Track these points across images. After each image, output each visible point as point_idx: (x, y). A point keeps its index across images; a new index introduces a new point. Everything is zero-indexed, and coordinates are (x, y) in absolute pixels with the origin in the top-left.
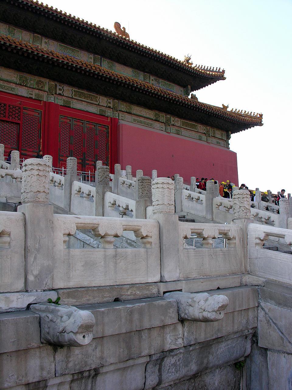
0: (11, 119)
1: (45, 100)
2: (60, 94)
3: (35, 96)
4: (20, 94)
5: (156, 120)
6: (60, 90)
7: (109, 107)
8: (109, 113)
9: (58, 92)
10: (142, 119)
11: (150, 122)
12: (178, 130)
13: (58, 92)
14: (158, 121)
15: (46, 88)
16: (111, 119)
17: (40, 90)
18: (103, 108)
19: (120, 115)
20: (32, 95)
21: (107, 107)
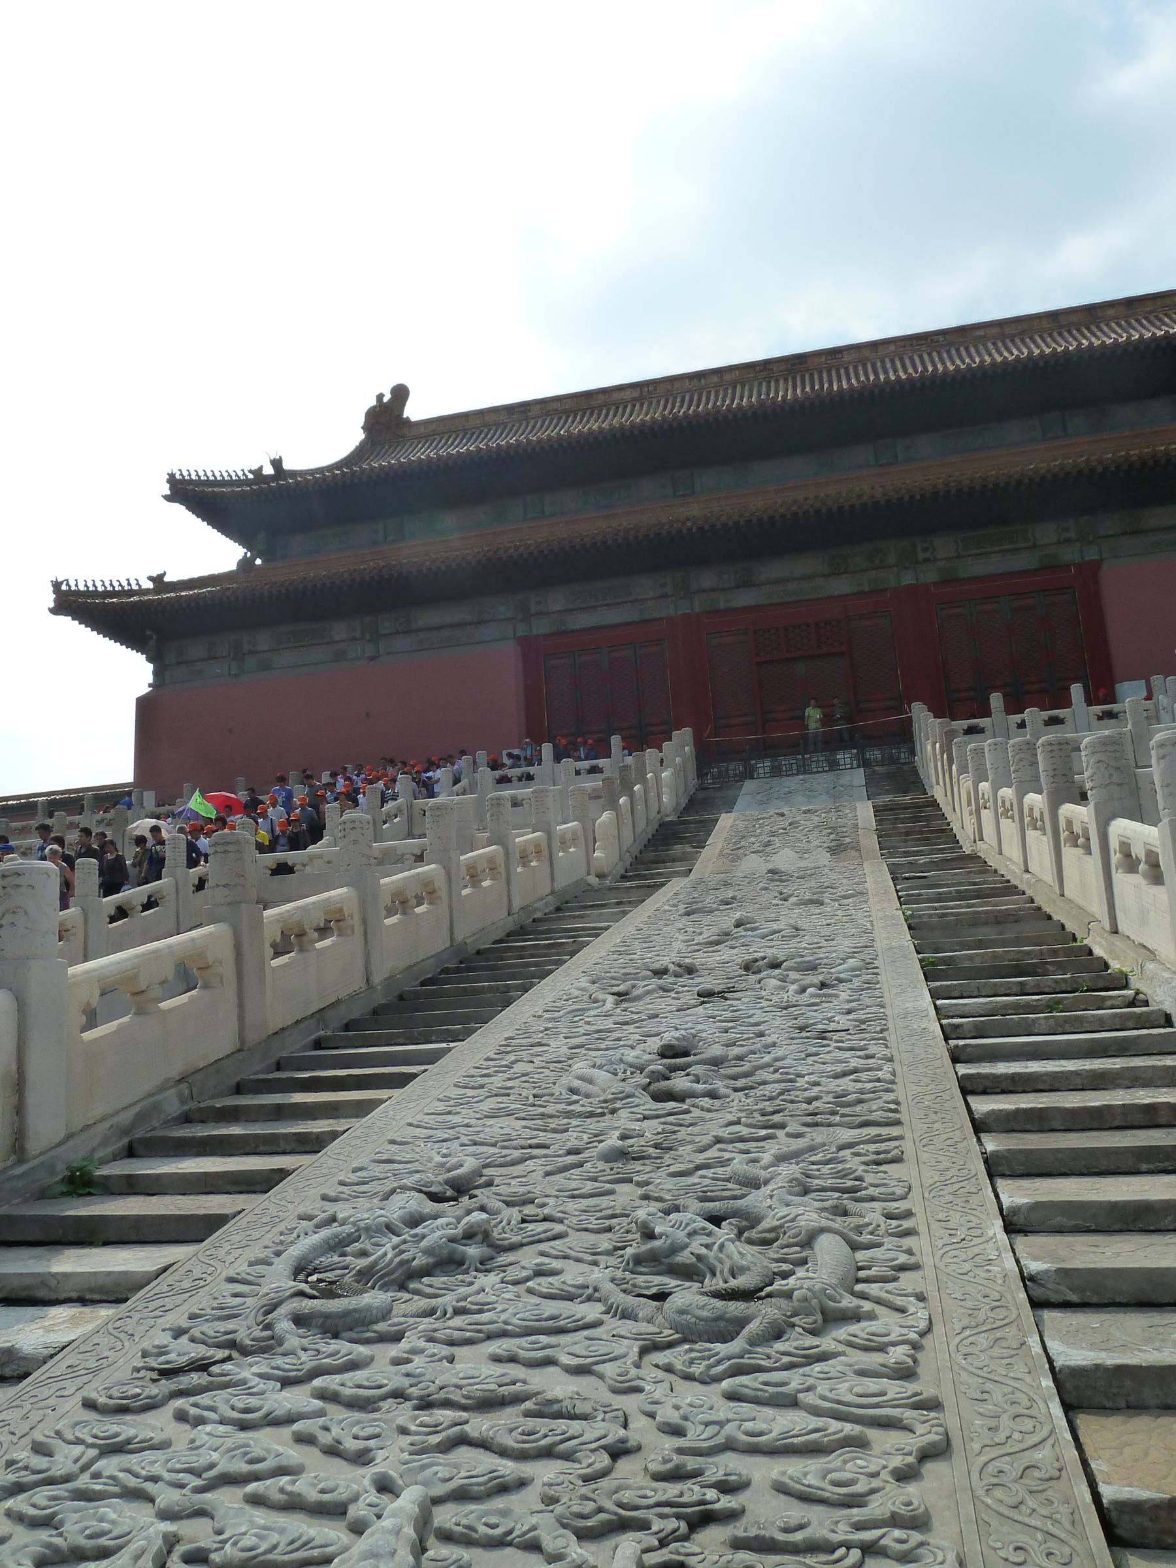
2: (926, 560)
6: (924, 550)
7: (1068, 541)
8: (1070, 555)
9: (921, 556)
13: (921, 556)
15: (892, 559)
17: (878, 568)
21: (1059, 543)
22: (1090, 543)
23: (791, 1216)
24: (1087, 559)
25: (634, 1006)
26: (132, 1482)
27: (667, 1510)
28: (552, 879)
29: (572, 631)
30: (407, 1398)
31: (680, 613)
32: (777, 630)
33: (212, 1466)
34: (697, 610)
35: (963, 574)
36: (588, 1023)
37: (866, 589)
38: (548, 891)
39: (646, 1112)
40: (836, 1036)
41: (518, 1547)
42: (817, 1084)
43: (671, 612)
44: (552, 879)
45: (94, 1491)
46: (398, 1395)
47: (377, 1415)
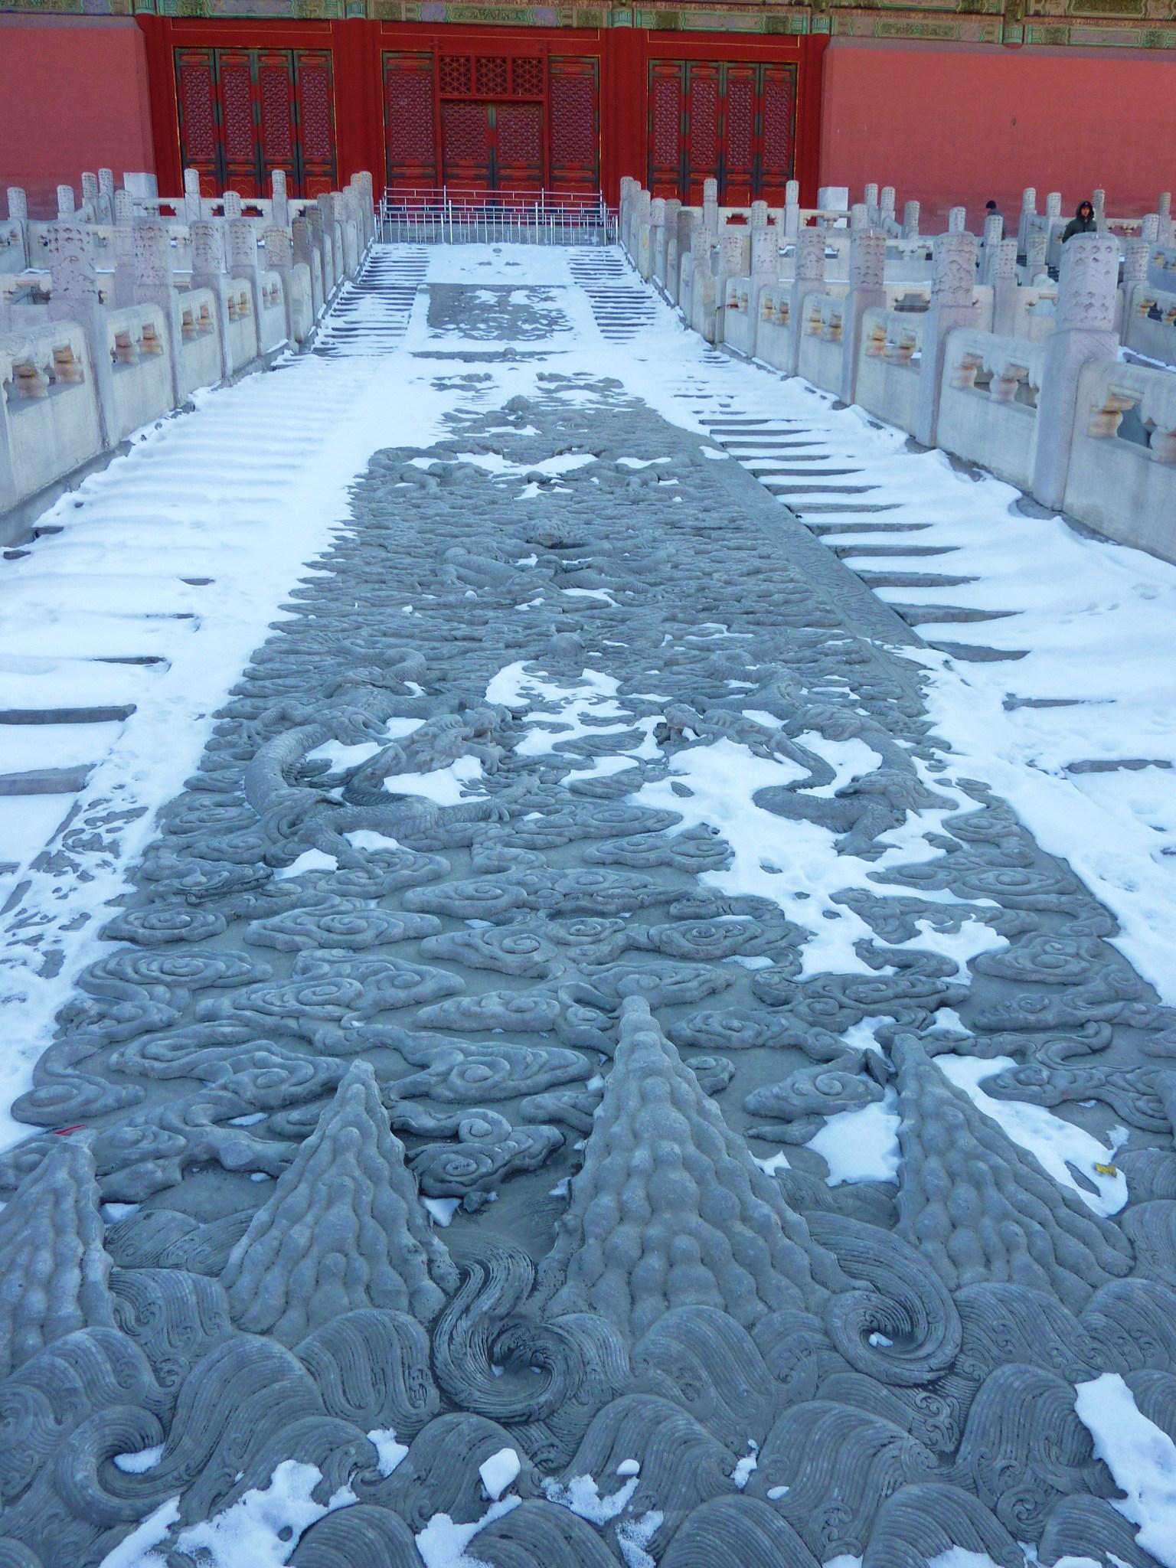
0: (520, 95)
1: (605, 25)
3: (579, 18)
4: (539, 23)
5: (967, 12)
10: (916, 20)
11: (946, 21)
12: (1057, 30)
14: (978, 13)
16: (805, 38)
18: (781, 12)
19: (836, 20)
20: (570, 17)
22: (822, 11)
23: (828, 714)
24: (815, 32)
25: (460, 490)
26: (269, 1020)
27: (907, 1000)
28: (258, 338)
29: (211, 19)
30: (534, 909)
31: (350, 16)
32: (504, 61)
33: (359, 995)
34: (372, 16)
35: (682, 25)
36: (418, 507)
37: (575, 25)
38: (254, 353)
39: (565, 606)
40: (714, 534)
41: (771, 1047)
42: (728, 583)
43: (340, 15)
44: (258, 338)
45: (224, 1035)
46: (520, 905)
47: (515, 926)
